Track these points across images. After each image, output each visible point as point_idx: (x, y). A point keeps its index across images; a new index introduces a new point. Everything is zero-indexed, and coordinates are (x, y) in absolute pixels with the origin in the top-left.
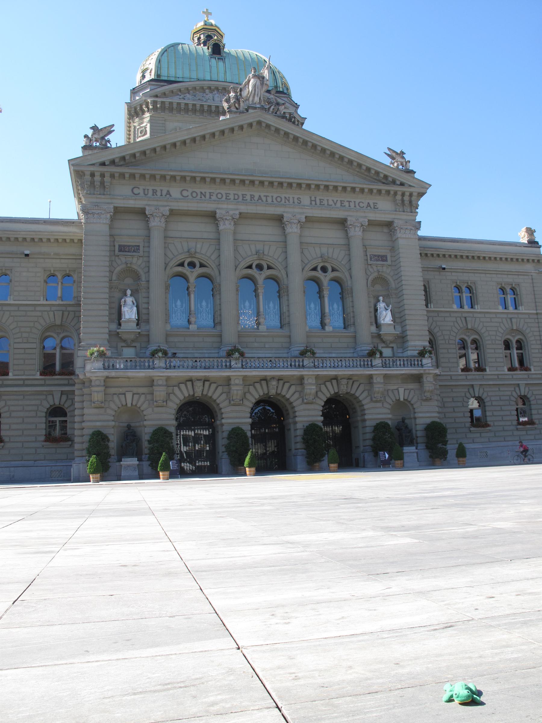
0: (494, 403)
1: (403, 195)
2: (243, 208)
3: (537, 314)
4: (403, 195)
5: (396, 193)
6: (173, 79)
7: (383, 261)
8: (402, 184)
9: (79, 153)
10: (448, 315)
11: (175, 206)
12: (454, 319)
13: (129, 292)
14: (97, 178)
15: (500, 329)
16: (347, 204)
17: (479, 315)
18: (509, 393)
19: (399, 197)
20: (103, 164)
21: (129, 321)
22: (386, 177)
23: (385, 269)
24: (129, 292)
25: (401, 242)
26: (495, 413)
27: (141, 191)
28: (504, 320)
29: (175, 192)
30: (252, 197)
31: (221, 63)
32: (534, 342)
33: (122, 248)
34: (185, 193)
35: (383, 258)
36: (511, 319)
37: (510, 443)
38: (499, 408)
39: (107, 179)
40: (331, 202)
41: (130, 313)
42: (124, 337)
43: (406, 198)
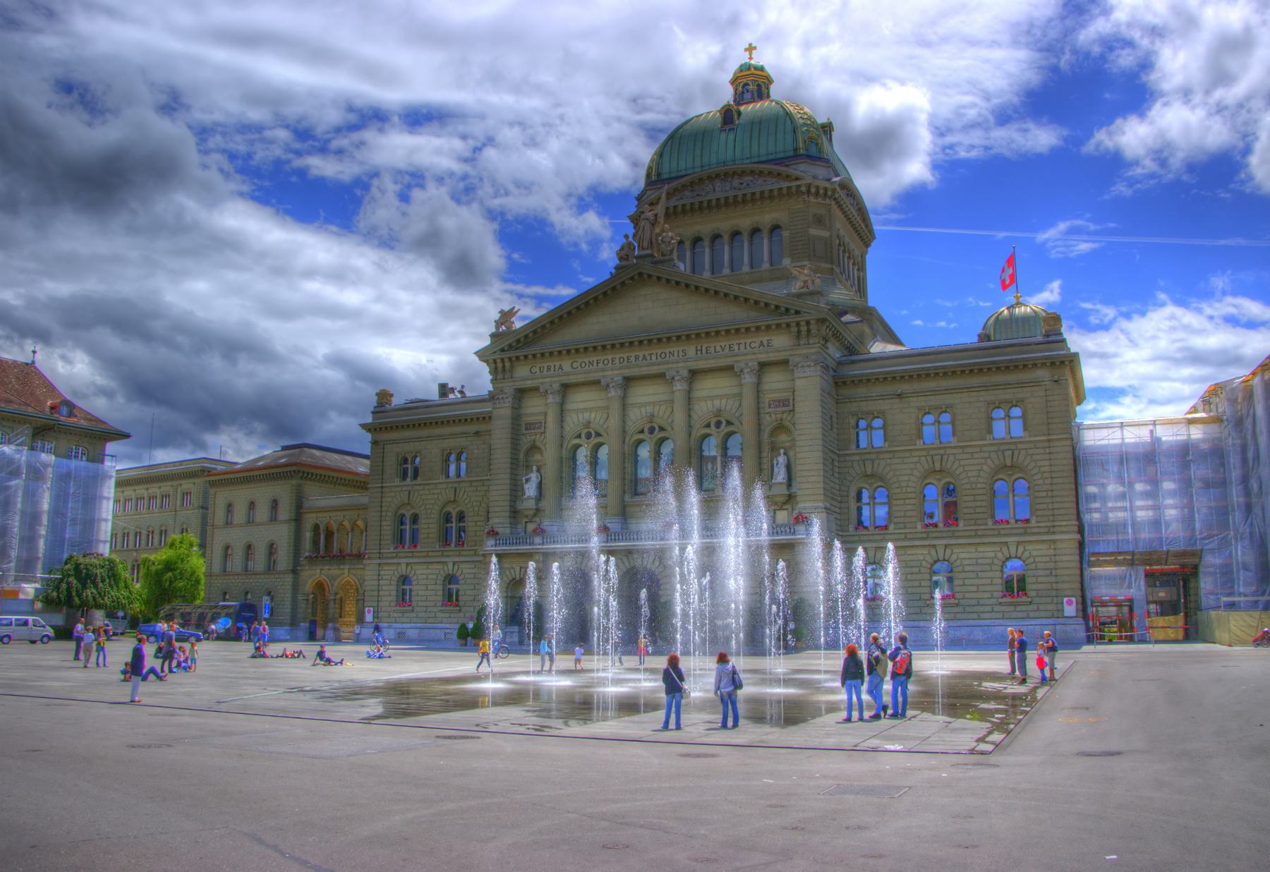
0: (967, 568)
1: (798, 324)
2: (627, 372)
3: (1049, 441)
4: (798, 324)
5: (788, 325)
6: (674, 175)
7: (784, 405)
8: (797, 312)
9: (488, 342)
10: (907, 454)
11: (566, 380)
12: (916, 459)
13: (535, 468)
14: (500, 365)
15: (985, 467)
16: (736, 347)
17: (954, 451)
18: (992, 555)
19: (794, 329)
20: (503, 350)
21: (529, 498)
22: (777, 307)
23: (785, 416)
24: (535, 468)
25: (798, 382)
26: (967, 582)
27: (537, 369)
28: (993, 455)
29: (566, 365)
30: (637, 358)
31: (731, 136)
32: (1041, 482)
33: (529, 426)
34: (575, 365)
35: (784, 402)
36: (1003, 451)
37: (987, 622)
38: (974, 575)
39: (507, 364)
40: (718, 349)
41: (530, 490)
42: (526, 513)
43: (804, 328)
